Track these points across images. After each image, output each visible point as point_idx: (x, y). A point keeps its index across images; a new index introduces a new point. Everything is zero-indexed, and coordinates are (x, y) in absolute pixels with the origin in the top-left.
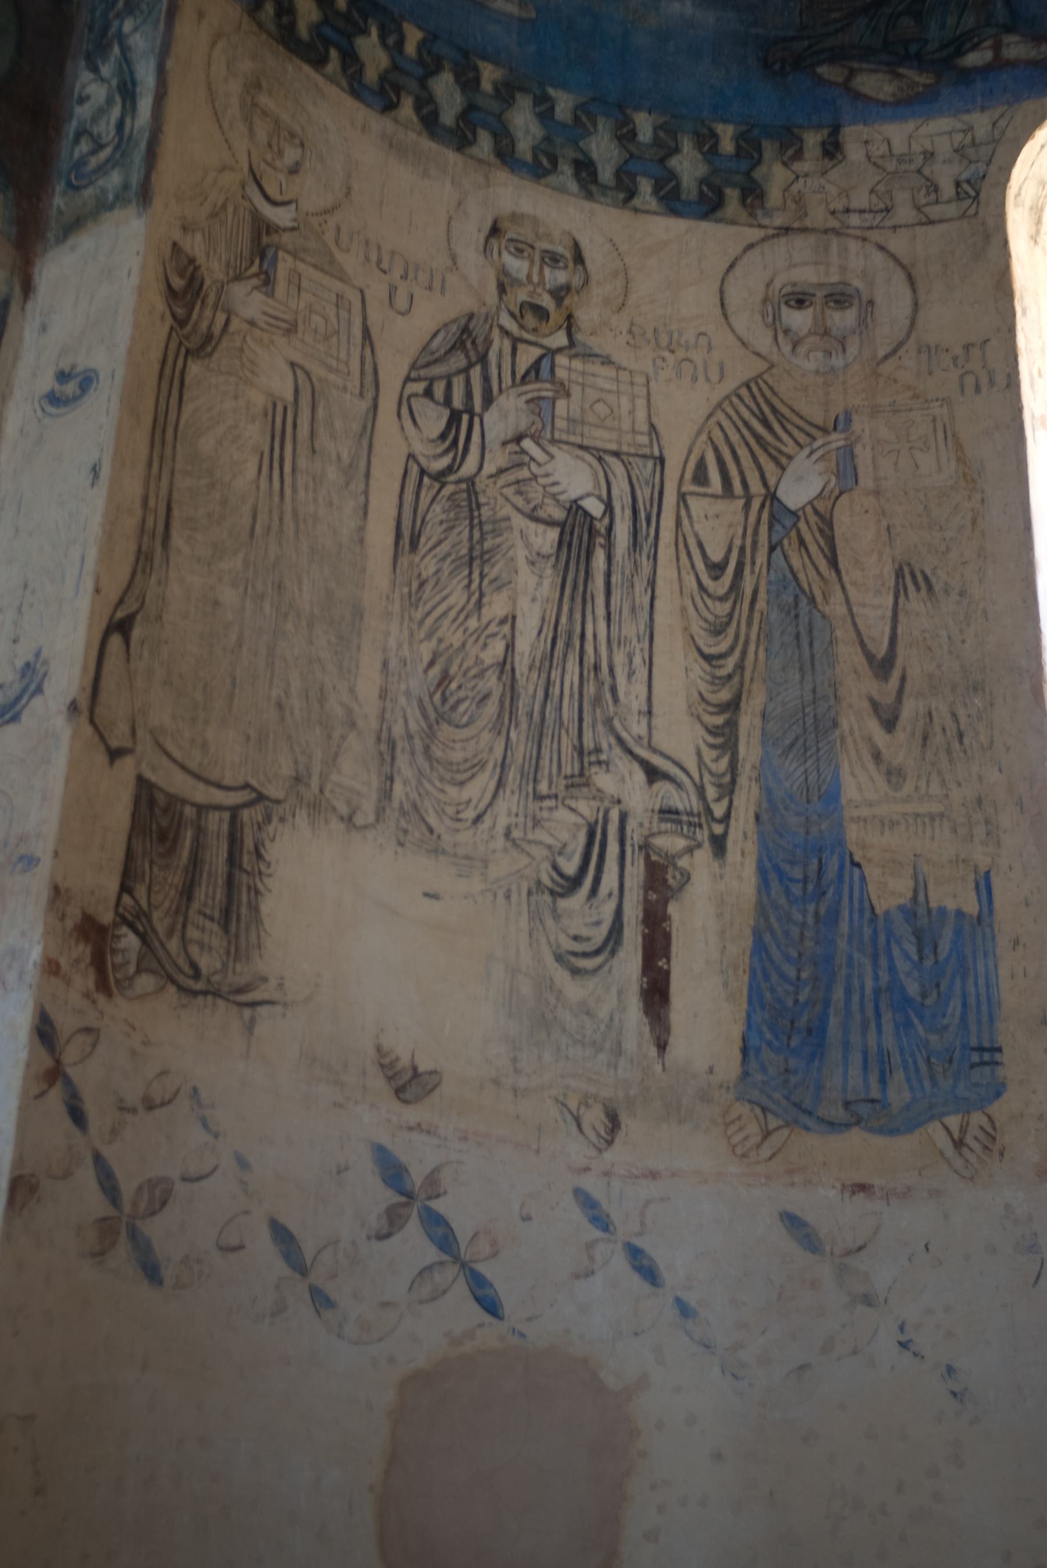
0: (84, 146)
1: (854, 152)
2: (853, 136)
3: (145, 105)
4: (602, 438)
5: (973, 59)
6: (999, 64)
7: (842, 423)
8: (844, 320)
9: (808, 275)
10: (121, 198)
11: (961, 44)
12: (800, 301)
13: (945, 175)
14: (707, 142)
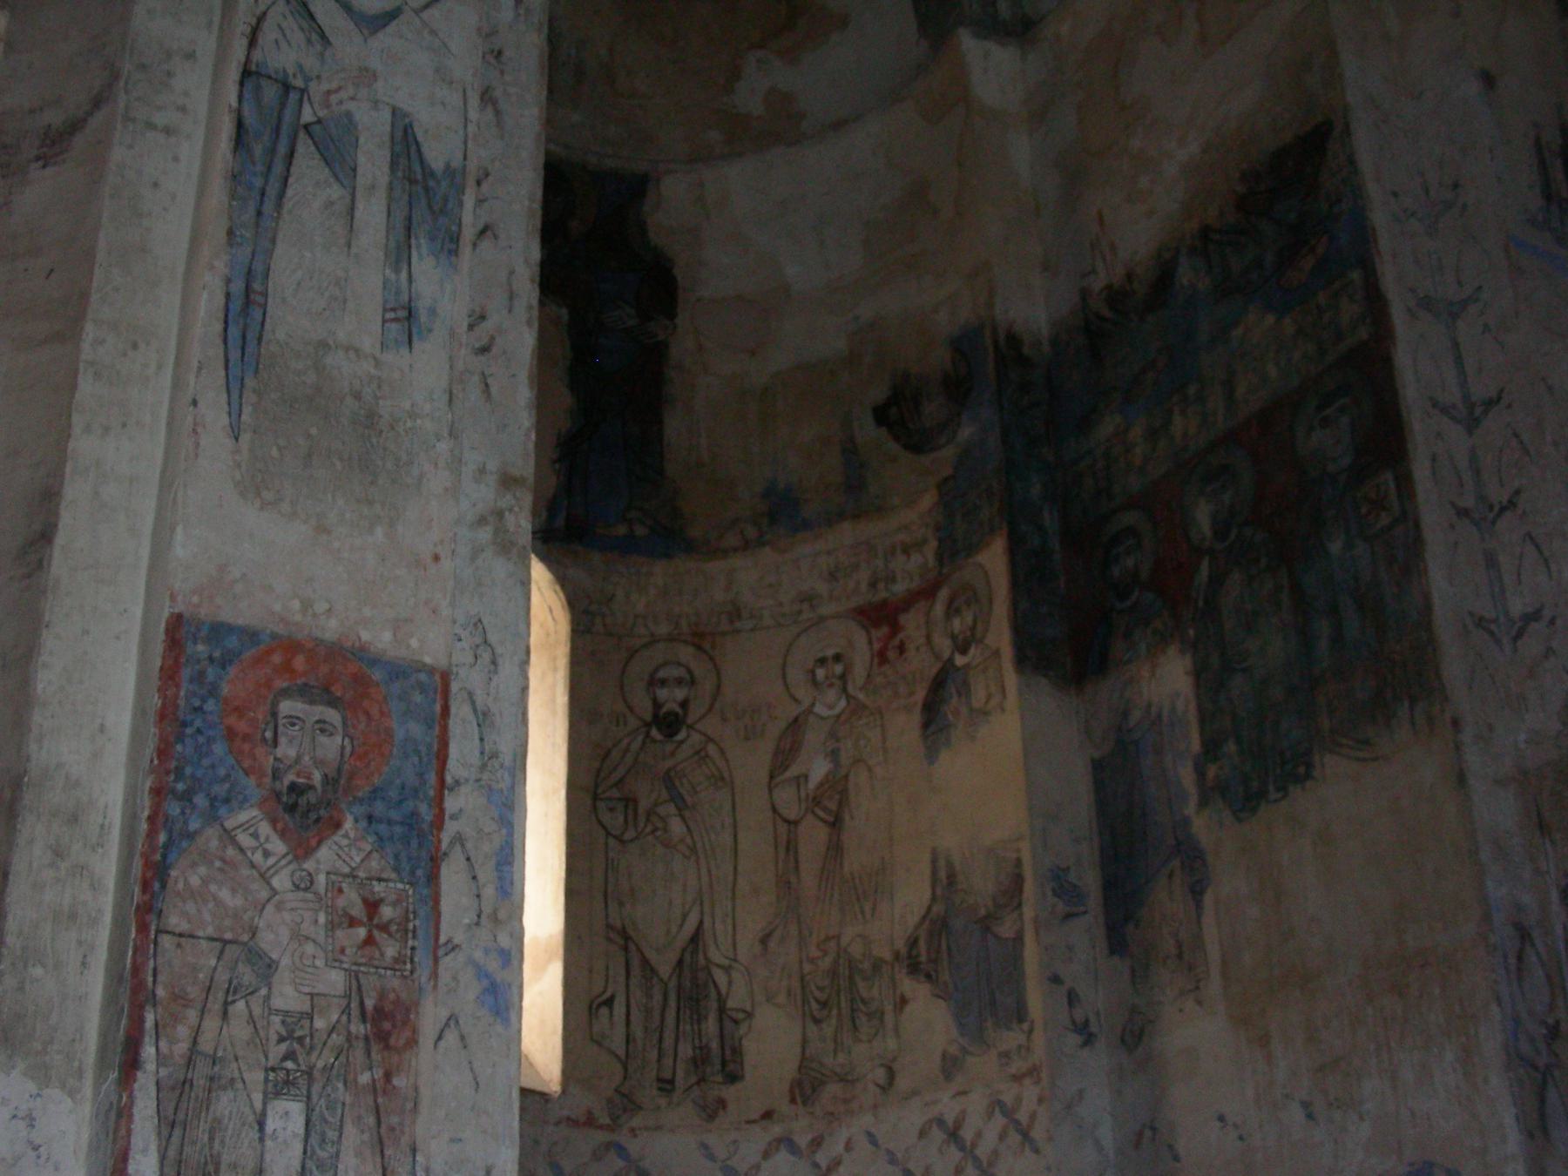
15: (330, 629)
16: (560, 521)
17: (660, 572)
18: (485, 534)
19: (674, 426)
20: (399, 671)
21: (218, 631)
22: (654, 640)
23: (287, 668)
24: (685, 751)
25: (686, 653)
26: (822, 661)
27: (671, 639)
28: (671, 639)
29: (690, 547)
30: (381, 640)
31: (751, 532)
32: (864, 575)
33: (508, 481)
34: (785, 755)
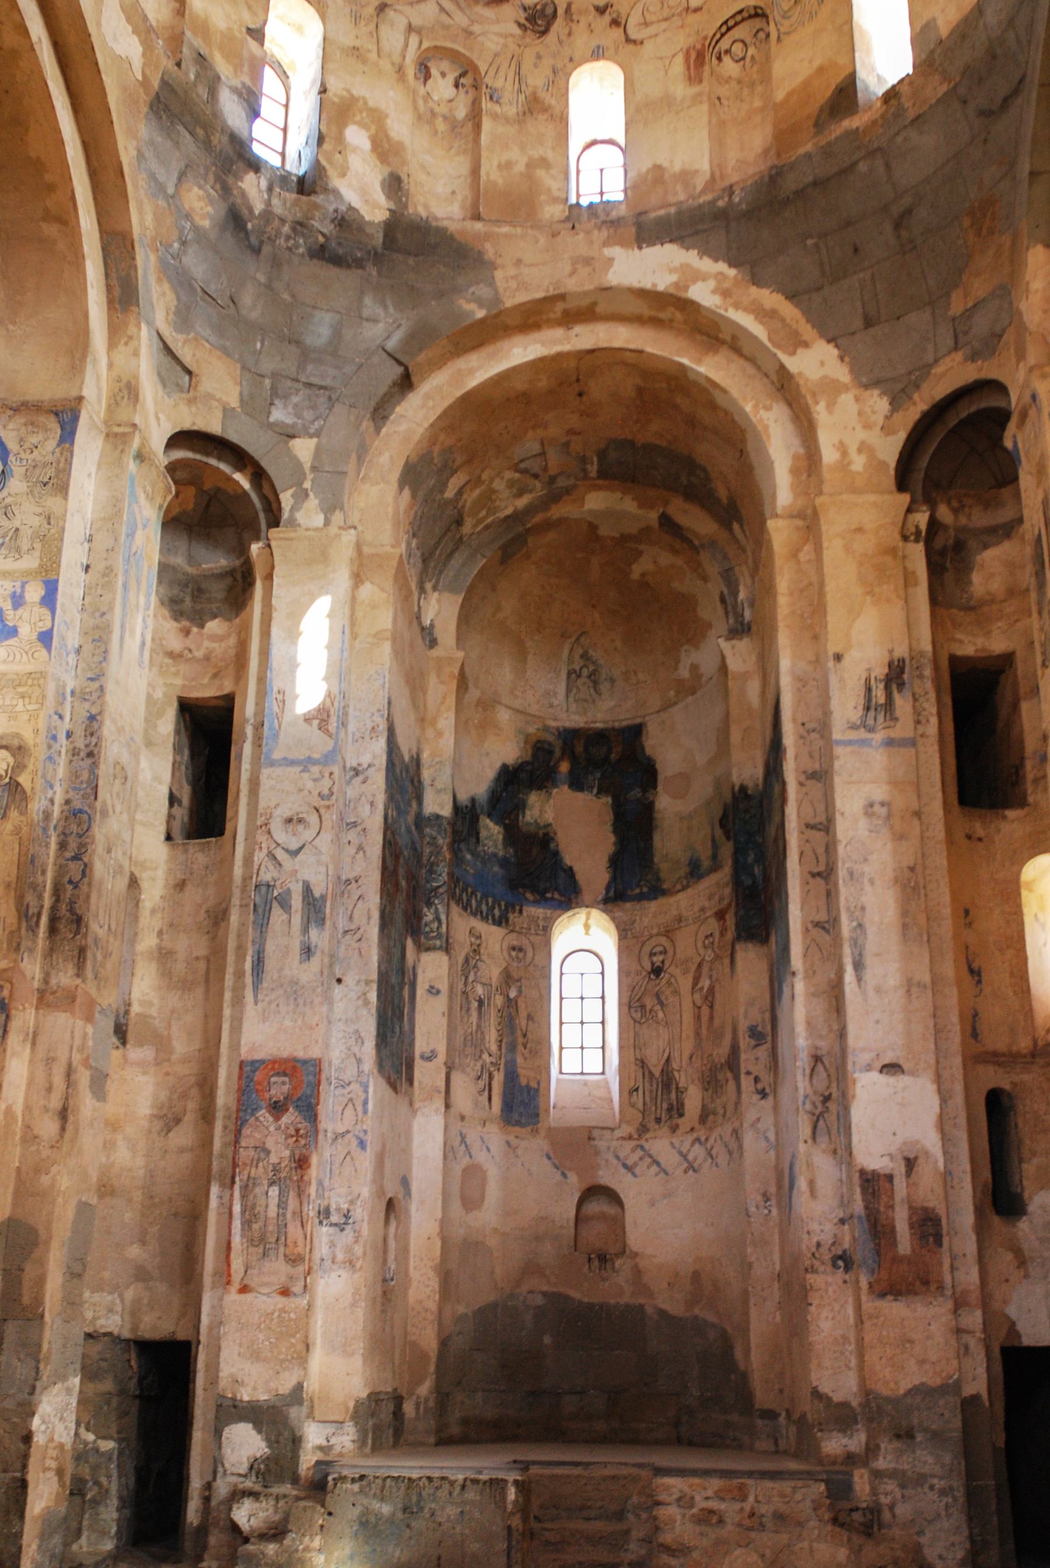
0: (427, 929)
1: (525, 913)
2: (525, 908)
3: (444, 927)
4: (483, 980)
5: (549, 895)
6: (553, 899)
7: (519, 980)
8: (521, 955)
9: (515, 943)
10: (440, 948)
11: (546, 891)
12: (514, 949)
13: (541, 923)
14: (500, 906)
15: (285, 1054)
16: (612, 893)
17: (653, 906)
18: (360, 1002)
19: (657, 839)
20: (305, 1062)
21: (253, 1062)
22: (651, 936)
23: (273, 1069)
24: (664, 981)
25: (663, 940)
26: (707, 937)
27: (658, 935)
28: (658, 935)
29: (664, 893)
30: (301, 1054)
31: (685, 882)
32: (717, 897)
33: (368, 982)
34: (696, 980)
